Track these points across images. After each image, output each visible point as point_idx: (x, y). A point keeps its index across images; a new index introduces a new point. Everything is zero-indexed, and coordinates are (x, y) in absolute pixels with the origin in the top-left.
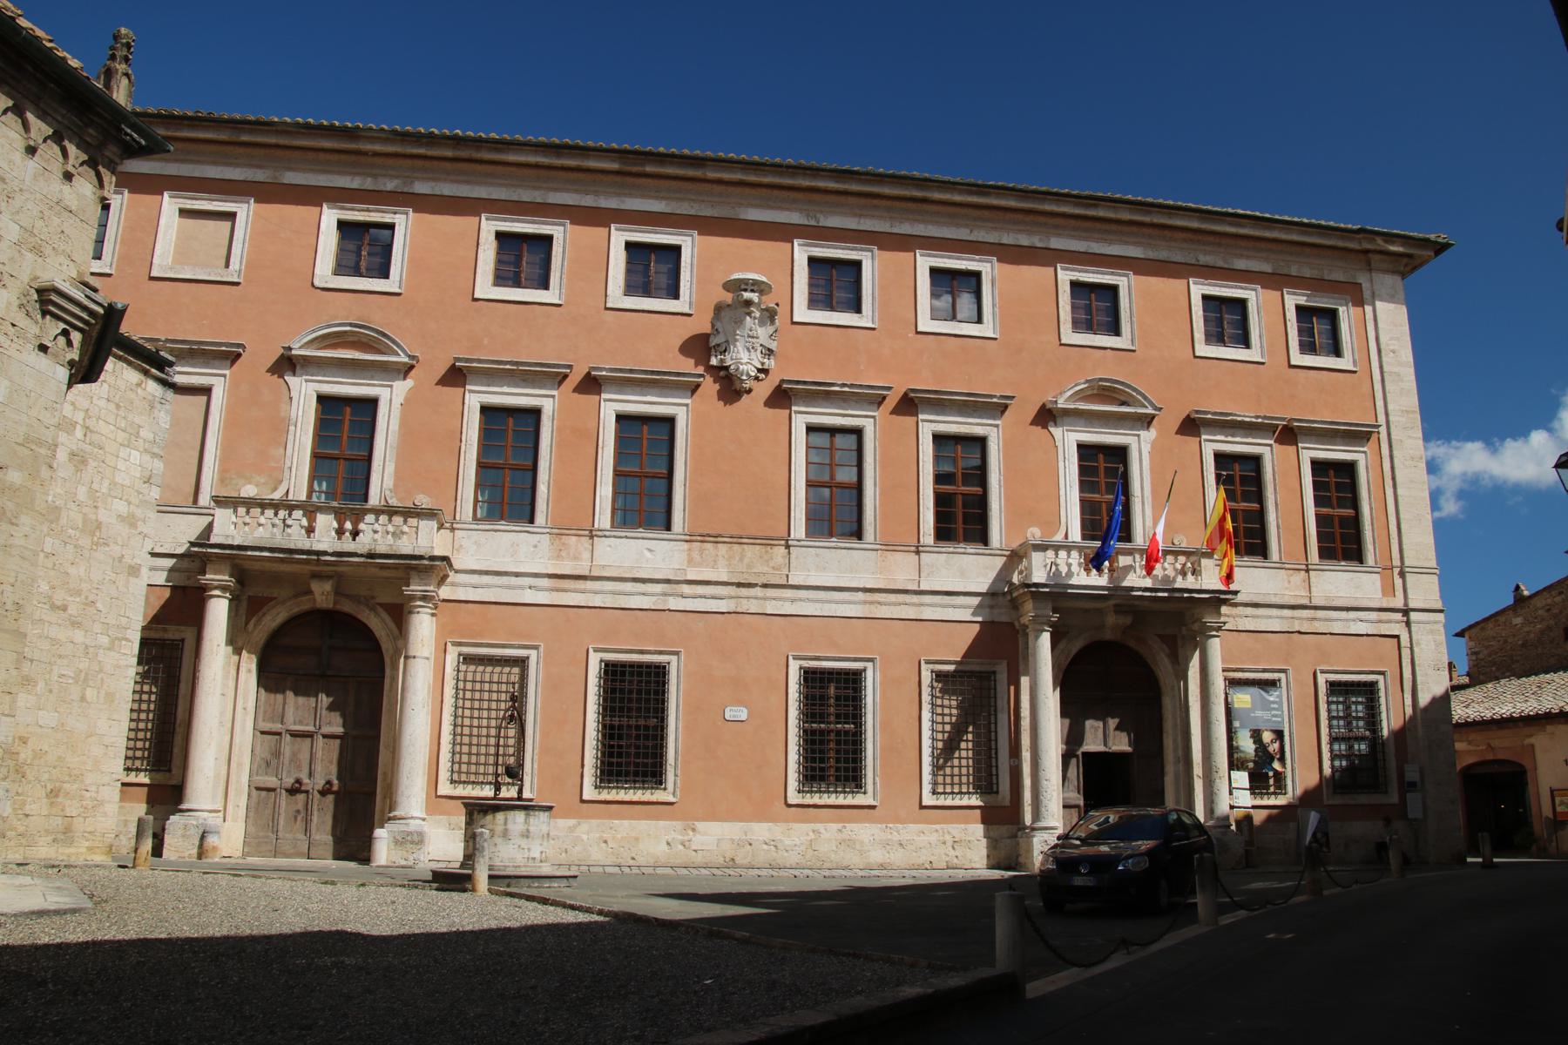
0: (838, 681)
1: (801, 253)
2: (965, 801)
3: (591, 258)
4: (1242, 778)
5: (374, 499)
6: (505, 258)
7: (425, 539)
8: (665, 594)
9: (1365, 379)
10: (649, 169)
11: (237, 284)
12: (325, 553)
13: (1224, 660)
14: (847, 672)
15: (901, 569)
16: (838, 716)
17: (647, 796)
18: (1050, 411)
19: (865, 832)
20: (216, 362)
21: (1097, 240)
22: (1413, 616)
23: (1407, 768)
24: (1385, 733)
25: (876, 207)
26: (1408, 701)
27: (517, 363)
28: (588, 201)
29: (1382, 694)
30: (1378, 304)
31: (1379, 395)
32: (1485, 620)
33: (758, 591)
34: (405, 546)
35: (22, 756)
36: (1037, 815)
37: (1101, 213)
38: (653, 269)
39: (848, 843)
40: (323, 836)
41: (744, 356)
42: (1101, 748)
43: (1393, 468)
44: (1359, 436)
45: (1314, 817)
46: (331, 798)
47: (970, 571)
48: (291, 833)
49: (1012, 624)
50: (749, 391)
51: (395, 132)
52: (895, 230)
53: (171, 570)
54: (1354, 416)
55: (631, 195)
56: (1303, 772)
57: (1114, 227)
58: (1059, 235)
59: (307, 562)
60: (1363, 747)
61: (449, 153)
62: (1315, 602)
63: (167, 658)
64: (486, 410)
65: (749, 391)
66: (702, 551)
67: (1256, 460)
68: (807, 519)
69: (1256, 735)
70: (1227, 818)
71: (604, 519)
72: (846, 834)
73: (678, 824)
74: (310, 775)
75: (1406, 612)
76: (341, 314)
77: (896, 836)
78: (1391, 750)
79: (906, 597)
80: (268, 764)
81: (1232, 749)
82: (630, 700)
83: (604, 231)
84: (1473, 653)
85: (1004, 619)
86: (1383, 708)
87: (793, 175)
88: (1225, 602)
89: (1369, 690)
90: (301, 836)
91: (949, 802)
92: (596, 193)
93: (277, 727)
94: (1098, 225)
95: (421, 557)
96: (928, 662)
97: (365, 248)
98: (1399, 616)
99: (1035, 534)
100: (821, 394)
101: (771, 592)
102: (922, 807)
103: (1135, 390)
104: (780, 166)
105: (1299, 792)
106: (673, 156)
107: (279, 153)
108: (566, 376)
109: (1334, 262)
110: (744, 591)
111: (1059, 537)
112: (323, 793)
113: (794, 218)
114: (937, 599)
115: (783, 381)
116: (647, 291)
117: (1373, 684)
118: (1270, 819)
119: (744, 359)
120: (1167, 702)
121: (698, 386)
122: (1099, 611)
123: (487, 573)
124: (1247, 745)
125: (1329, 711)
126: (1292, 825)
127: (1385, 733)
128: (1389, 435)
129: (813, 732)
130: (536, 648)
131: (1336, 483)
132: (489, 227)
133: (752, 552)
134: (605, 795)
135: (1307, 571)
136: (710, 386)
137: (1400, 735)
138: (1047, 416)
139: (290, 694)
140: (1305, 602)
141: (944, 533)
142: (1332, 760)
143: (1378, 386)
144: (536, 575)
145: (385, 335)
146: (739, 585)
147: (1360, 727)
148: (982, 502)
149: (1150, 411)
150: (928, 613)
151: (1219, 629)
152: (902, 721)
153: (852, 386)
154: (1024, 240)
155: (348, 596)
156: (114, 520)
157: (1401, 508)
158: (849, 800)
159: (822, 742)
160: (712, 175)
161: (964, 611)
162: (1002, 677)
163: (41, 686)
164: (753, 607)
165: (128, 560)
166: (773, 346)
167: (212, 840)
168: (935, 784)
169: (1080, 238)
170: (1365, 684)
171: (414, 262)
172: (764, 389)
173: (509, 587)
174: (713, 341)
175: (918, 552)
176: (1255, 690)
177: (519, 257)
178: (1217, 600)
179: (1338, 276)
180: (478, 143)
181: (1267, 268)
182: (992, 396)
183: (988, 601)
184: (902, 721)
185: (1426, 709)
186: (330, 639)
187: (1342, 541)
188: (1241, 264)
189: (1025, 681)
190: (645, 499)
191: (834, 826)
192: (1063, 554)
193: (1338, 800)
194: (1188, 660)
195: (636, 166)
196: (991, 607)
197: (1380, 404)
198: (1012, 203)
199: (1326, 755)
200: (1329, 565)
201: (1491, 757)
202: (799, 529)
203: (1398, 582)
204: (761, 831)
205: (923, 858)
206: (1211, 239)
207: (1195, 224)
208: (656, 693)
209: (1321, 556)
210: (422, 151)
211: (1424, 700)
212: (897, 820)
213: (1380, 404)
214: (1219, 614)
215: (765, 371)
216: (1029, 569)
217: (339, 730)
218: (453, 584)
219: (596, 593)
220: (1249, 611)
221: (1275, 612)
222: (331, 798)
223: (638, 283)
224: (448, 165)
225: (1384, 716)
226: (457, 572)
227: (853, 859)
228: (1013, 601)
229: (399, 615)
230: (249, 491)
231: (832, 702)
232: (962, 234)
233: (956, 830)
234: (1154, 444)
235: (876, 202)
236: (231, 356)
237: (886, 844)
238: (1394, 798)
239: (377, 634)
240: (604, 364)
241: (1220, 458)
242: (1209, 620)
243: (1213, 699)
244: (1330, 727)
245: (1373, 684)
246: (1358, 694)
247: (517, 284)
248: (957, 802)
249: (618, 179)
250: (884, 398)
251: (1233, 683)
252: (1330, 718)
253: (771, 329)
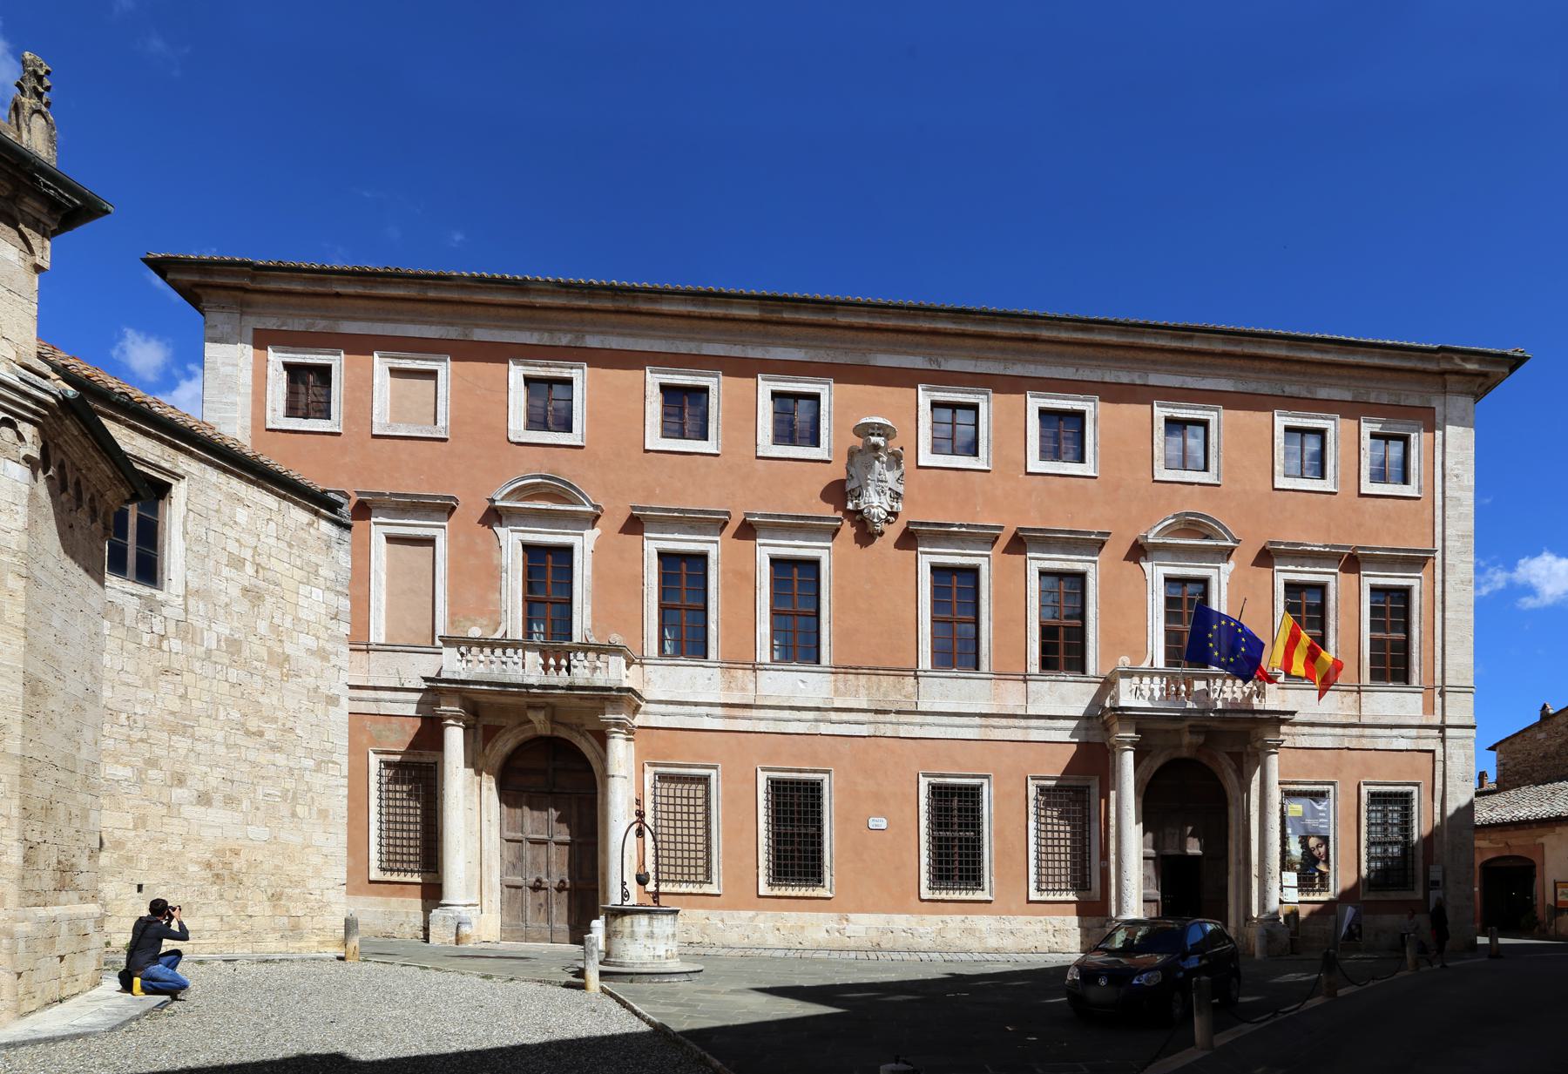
0: (960, 795)
1: (925, 398)
2: (1064, 897)
3: (745, 406)
4: (1291, 878)
5: (577, 637)
6: (671, 410)
7: (614, 672)
9: (1429, 506)
10: (787, 316)
11: (445, 440)
13: (1280, 774)
14: (967, 787)
15: (1011, 697)
16: (960, 825)
17: (810, 892)
18: (1141, 546)
19: (983, 922)
20: (436, 515)
21: (1191, 375)
22: (1449, 732)
23: (1432, 868)
24: (1416, 837)
25: (991, 349)
26: (1438, 810)
27: (683, 511)
28: (736, 351)
29: (1415, 803)
30: (1448, 428)
31: (1439, 520)
32: (1515, 736)
33: (892, 717)
34: (600, 680)
35: (236, 866)
36: (1120, 910)
37: (1195, 345)
38: (796, 421)
39: (969, 931)
40: (562, 925)
41: (875, 500)
42: (1177, 852)
43: (1443, 592)
44: (1415, 561)
45: (1350, 911)
46: (565, 894)
47: (1069, 697)
48: (537, 923)
49: (1103, 745)
50: (881, 534)
51: (558, 283)
52: (1008, 372)
53: (419, 703)
54: (1414, 542)
55: (774, 345)
56: (1342, 875)
57: (1207, 360)
58: (1157, 371)
60: (1396, 850)
61: (609, 305)
62: (1365, 721)
63: (417, 775)
64: (663, 555)
65: (881, 534)
66: (846, 682)
67: (1322, 588)
68: (933, 652)
69: (1304, 841)
70: (1277, 913)
71: (764, 655)
72: (968, 924)
73: (835, 916)
74: (548, 876)
75: (1442, 728)
76: (532, 467)
77: (1008, 926)
78: (1419, 853)
79: (1011, 719)
80: (514, 866)
81: (1284, 853)
82: (792, 812)
83: (751, 381)
84: (1501, 765)
85: (1098, 740)
86: (1415, 816)
87: (915, 317)
88: (1284, 722)
89: (1404, 800)
90: (544, 925)
91: (1051, 897)
92: (743, 344)
93: (519, 836)
94: (1193, 359)
95: (610, 689)
96: (1033, 778)
97: (549, 406)
98: (1435, 732)
99: (1125, 661)
100: (942, 535)
101: (903, 718)
102: (1029, 902)
103: (1217, 523)
104: (901, 308)
105: (1339, 890)
106: (805, 300)
107: (465, 309)
108: (726, 523)
109: (1409, 383)
110: (881, 718)
111: (1146, 665)
112: (559, 890)
113: (918, 362)
114: (1041, 722)
115: (909, 523)
116: (791, 440)
117: (1408, 795)
118: (1312, 914)
119: (875, 503)
120: (1232, 811)
121: (838, 530)
122: (1177, 731)
124: (1295, 849)
125: (1369, 818)
126: (1332, 917)
127: (1416, 837)
128: (1444, 559)
129: (940, 839)
130: (715, 767)
131: (1393, 608)
132: (654, 380)
133: (887, 682)
134: (776, 892)
135: (1359, 692)
136: (848, 530)
137: (1428, 841)
138: (1139, 552)
139: (526, 809)
140: (1355, 721)
141: (1049, 663)
142: (1369, 862)
143: (1438, 512)
145: (571, 486)
146: (877, 712)
147: (1395, 834)
148: (1082, 631)
149: (1230, 543)
150: (1034, 735)
151: (1278, 746)
152: (1013, 830)
153: (968, 526)
154: (1125, 378)
157: (1447, 631)
158: (970, 896)
159: (947, 847)
160: (843, 320)
161: (1063, 733)
162: (1095, 791)
163: (245, 804)
164: (889, 731)
165: (323, 689)
166: (901, 489)
167: (465, 929)
168: (1039, 882)
169: (1176, 373)
170: (1401, 794)
171: (593, 417)
172: (893, 532)
174: (849, 487)
175: (1025, 681)
176: (1307, 801)
177: (682, 409)
178: (1278, 719)
179: (1415, 401)
180: (631, 292)
181: (1348, 396)
182: (1090, 533)
183: (1084, 724)
184: (1013, 830)
185: (1452, 817)
186: (550, 762)
187: (1392, 664)
188: (1323, 393)
189: (1113, 794)
190: (798, 639)
191: (960, 917)
192: (1146, 680)
193: (1372, 896)
194: (1252, 774)
195: (777, 313)
196: (1087, 729)
197: (1438, 529)
198: (1113, 339)
199: (1364, 858)
200: (1379, 685)
201: (1507, 853)
202: (926, 662)
203: (1438, 700)
204: (900, 921)
205: (1030, 943)
206: (1297, 368)
207: (1283, 352)
208: (813, 805)
209: (1373, 678)
210: (584, 303)
211: (1450, 811)
212: (1009, 912)
213: (1438, 529)
214: (1279, 733)
215: (894, 514)
216: (1117, 694)
217: (567, 838)
220: (1306, 730)
221: (1328, 730)
222: (565, 894)
223: (785, 433)
224: (613, 318)
225: (1415, 822)
227: (972, 943)
228: (1104, 722)
229: (602, 738)
230: (475, 632)
231: (955, 811)
232: (1068, 373)
233: (1057, 921)
234: (1232, 575)
235: (990, 343)
236: (446, 509)
237: (1000, 932)
240: (760, 509)
241: (1290, 587)
242: (1270, 738)
243: (1269, 809)
244: (1369, 833)
245: (1408, 795)
246: (1396, 803)
247: (682, 436)
248: (1057, 898)
249: (761, 327)
250: (997, 538)
251: (1288, 795)
252: (1369, 825)
253: (897, 473)
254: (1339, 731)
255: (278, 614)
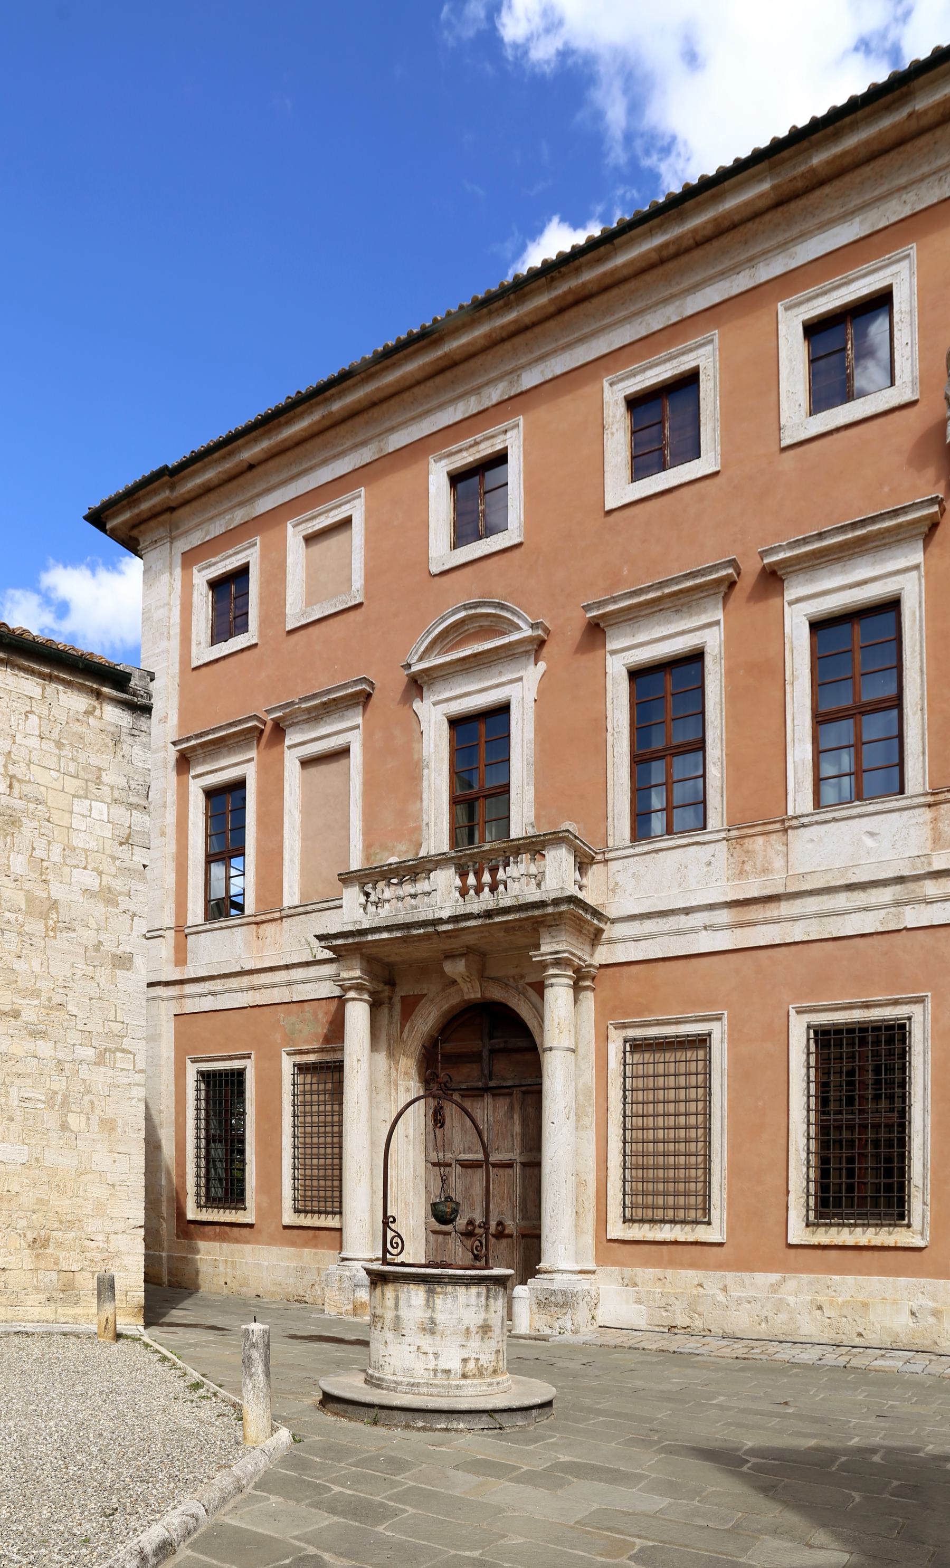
12: (440, 921)
59: (427, 936)
123: (649, 916)
144: (711, 907)
155: (495, 979)
156: (79, 897)
173: (678, 933)
218: (611, 941)
219: (794, 919)
226: (614, 921)
239: (530, 1026)
255: (41, 844)
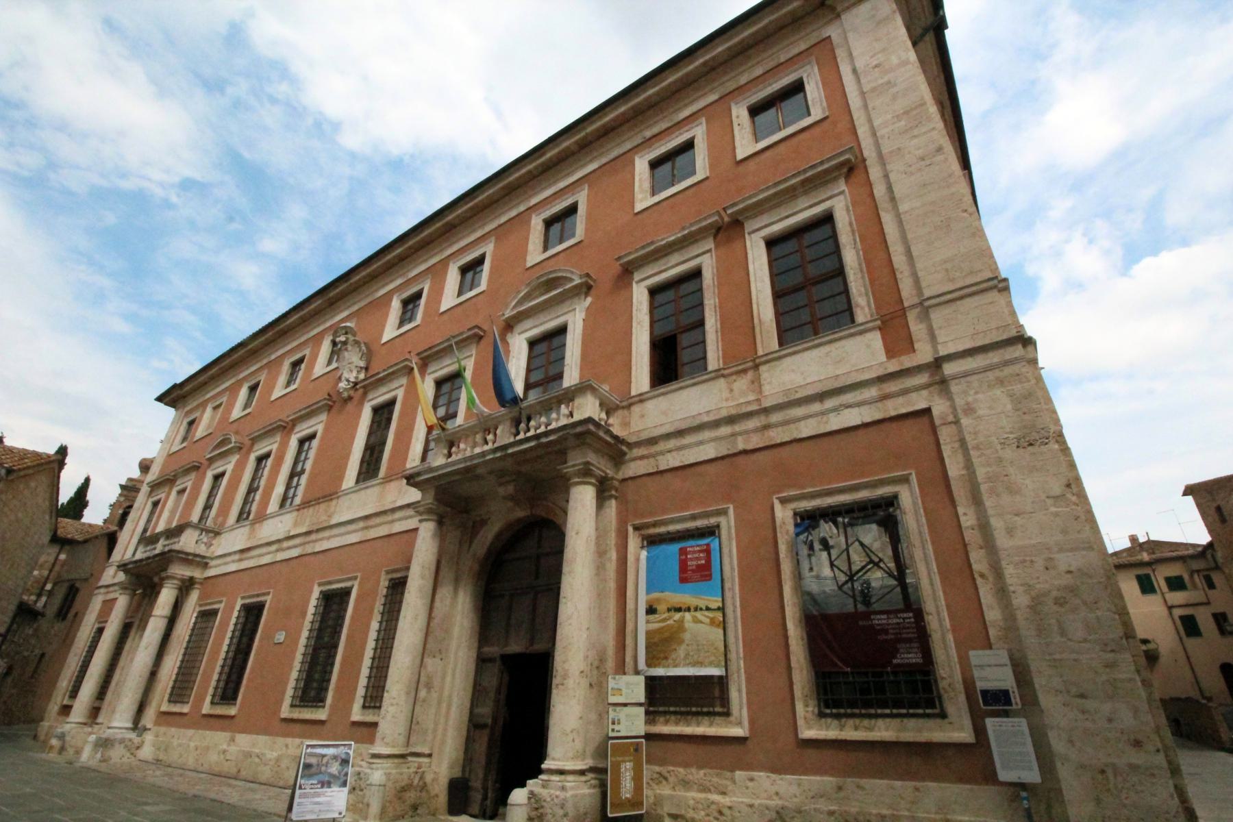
8: (277, 551)
62: (767, 403)
98: (923, 379)
220: (672, 443)
221: (707, 434)
238: (959, 731)
254: (725, 430)
